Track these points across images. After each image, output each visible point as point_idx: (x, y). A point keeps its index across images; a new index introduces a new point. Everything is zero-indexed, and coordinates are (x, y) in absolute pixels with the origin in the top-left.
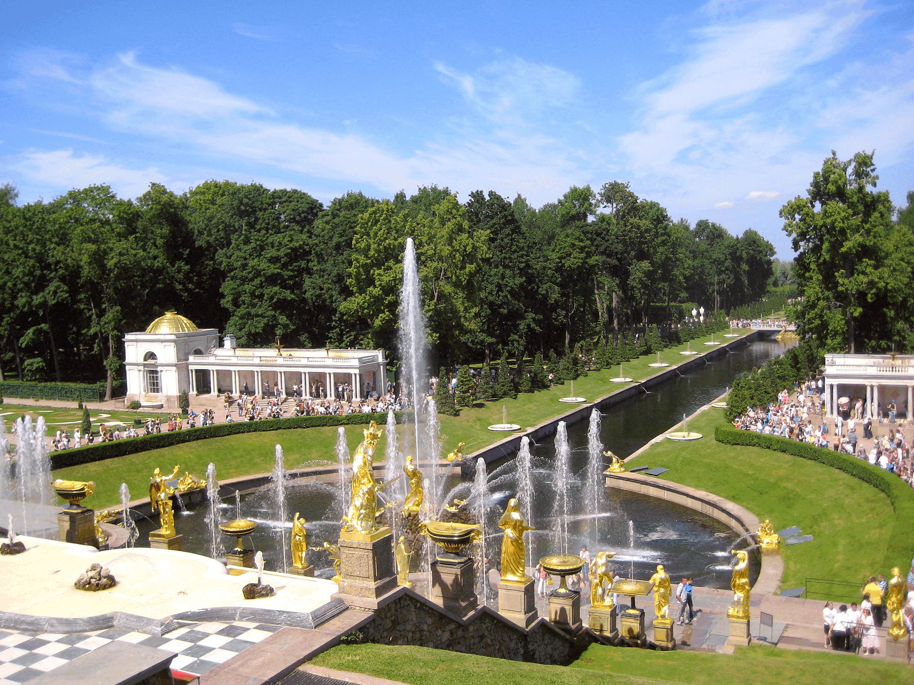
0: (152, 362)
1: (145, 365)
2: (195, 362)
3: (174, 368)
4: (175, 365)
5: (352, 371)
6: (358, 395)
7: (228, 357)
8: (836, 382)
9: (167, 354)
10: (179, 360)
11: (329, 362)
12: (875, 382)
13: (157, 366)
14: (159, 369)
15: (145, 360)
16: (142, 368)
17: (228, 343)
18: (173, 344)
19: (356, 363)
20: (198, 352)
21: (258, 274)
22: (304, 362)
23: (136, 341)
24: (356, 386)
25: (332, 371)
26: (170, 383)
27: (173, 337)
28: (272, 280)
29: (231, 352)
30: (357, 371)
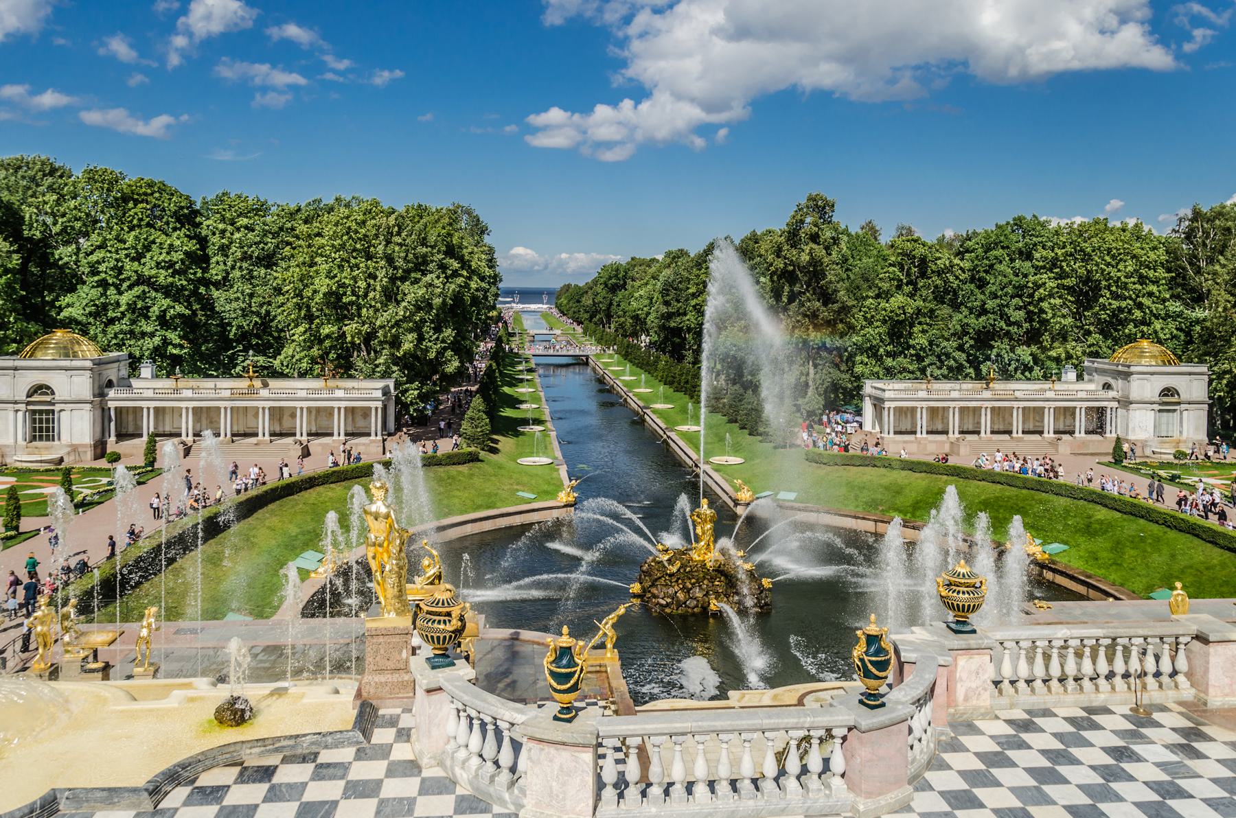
0: (48, 398)
1: (28, 403)
2: (116, 398)
3: (89, 406)
4: (91, 403)
5: (373, 404)
6: (379, 433)
7: (149, 388)
8: (893, 405)
9: (73, 385)
10: (94, 396)
11: (340, 394)
12: (925, 404)
13: (54, 404)
14: (57, 408)
15: (28, 396)
16: (23, 407)
17: (146, 370)
18: (88, 373)
19: (379, 394)
20: (110, 384)
21: (141, 280)
22: (303, 394)
23: (16, 369)
24: (375, 422)
25: (343, 404)
26: (77, 428)
27: (89, 364)
28: (167, 291)
29: (168, 383)
30: (380, 404)
